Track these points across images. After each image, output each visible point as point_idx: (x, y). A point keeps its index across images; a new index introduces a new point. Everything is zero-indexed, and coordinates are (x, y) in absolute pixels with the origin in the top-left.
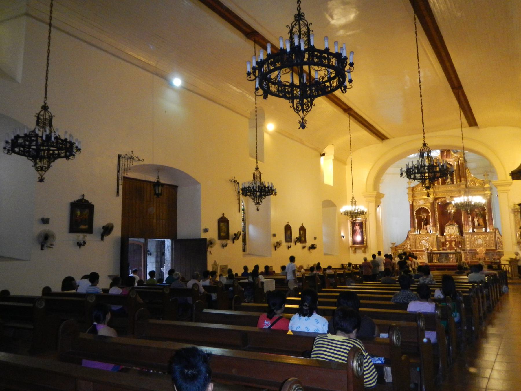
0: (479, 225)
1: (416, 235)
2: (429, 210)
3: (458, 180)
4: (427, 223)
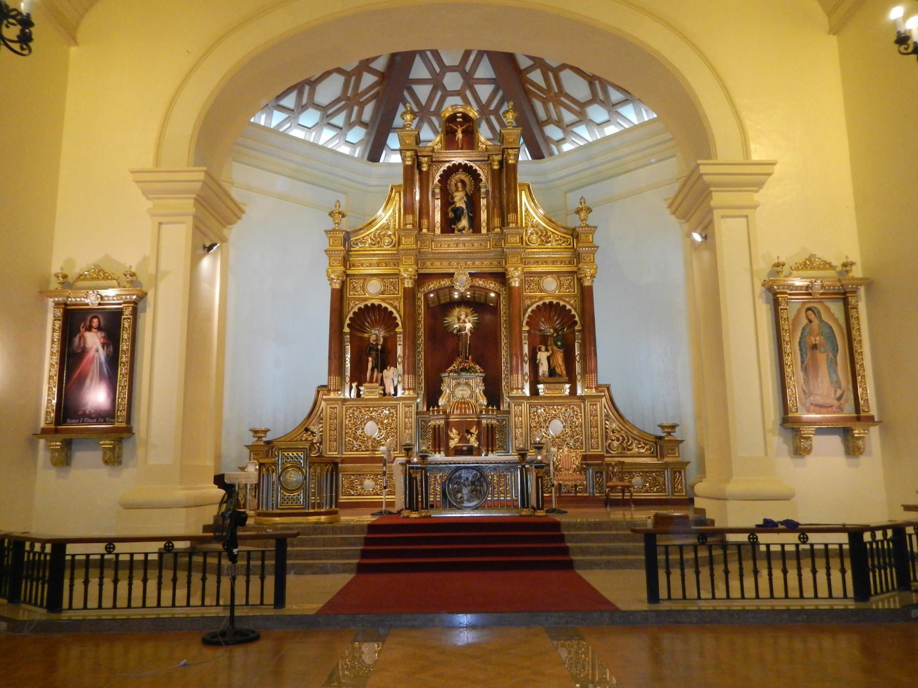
0: (552, 372)
1: (344, 400)
2: (396, 314)
3: (497, 221)
4: (385, 359)
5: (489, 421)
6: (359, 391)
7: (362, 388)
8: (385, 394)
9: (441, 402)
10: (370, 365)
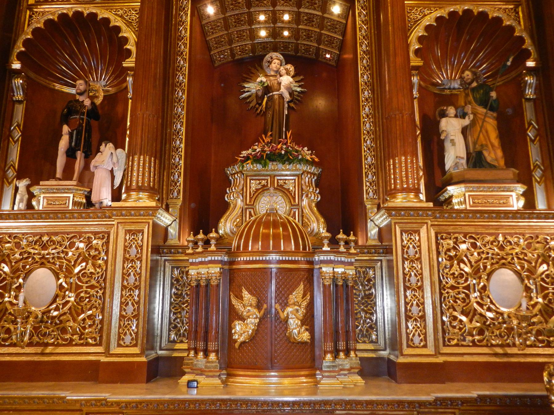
0: (476, 160)
5: (340, 270)
6: (31, 196)
7: (35, 190)
8: (89, 203)
9: (226, 226)
10: (63, 144)
